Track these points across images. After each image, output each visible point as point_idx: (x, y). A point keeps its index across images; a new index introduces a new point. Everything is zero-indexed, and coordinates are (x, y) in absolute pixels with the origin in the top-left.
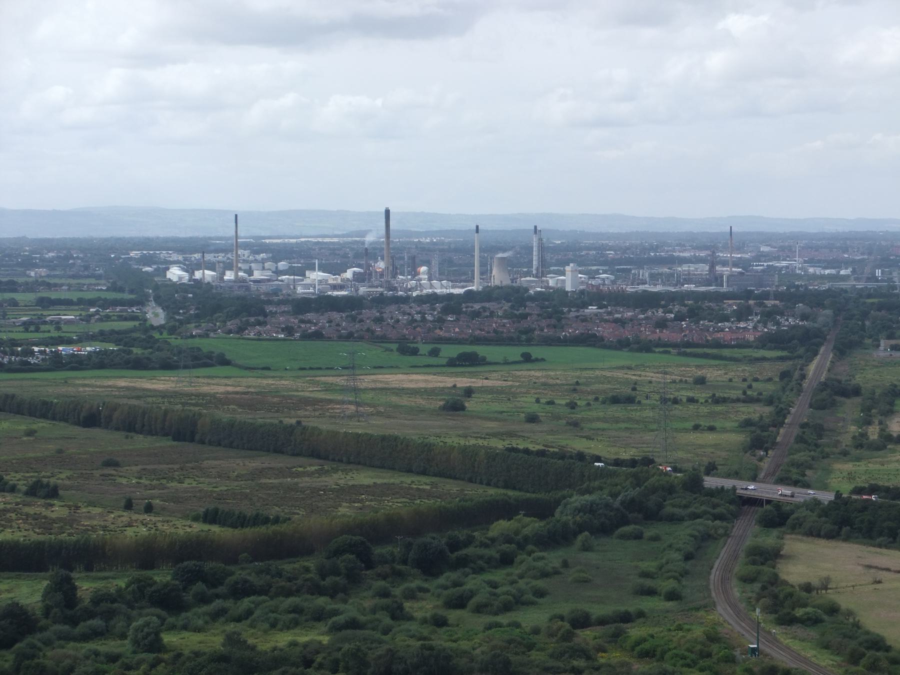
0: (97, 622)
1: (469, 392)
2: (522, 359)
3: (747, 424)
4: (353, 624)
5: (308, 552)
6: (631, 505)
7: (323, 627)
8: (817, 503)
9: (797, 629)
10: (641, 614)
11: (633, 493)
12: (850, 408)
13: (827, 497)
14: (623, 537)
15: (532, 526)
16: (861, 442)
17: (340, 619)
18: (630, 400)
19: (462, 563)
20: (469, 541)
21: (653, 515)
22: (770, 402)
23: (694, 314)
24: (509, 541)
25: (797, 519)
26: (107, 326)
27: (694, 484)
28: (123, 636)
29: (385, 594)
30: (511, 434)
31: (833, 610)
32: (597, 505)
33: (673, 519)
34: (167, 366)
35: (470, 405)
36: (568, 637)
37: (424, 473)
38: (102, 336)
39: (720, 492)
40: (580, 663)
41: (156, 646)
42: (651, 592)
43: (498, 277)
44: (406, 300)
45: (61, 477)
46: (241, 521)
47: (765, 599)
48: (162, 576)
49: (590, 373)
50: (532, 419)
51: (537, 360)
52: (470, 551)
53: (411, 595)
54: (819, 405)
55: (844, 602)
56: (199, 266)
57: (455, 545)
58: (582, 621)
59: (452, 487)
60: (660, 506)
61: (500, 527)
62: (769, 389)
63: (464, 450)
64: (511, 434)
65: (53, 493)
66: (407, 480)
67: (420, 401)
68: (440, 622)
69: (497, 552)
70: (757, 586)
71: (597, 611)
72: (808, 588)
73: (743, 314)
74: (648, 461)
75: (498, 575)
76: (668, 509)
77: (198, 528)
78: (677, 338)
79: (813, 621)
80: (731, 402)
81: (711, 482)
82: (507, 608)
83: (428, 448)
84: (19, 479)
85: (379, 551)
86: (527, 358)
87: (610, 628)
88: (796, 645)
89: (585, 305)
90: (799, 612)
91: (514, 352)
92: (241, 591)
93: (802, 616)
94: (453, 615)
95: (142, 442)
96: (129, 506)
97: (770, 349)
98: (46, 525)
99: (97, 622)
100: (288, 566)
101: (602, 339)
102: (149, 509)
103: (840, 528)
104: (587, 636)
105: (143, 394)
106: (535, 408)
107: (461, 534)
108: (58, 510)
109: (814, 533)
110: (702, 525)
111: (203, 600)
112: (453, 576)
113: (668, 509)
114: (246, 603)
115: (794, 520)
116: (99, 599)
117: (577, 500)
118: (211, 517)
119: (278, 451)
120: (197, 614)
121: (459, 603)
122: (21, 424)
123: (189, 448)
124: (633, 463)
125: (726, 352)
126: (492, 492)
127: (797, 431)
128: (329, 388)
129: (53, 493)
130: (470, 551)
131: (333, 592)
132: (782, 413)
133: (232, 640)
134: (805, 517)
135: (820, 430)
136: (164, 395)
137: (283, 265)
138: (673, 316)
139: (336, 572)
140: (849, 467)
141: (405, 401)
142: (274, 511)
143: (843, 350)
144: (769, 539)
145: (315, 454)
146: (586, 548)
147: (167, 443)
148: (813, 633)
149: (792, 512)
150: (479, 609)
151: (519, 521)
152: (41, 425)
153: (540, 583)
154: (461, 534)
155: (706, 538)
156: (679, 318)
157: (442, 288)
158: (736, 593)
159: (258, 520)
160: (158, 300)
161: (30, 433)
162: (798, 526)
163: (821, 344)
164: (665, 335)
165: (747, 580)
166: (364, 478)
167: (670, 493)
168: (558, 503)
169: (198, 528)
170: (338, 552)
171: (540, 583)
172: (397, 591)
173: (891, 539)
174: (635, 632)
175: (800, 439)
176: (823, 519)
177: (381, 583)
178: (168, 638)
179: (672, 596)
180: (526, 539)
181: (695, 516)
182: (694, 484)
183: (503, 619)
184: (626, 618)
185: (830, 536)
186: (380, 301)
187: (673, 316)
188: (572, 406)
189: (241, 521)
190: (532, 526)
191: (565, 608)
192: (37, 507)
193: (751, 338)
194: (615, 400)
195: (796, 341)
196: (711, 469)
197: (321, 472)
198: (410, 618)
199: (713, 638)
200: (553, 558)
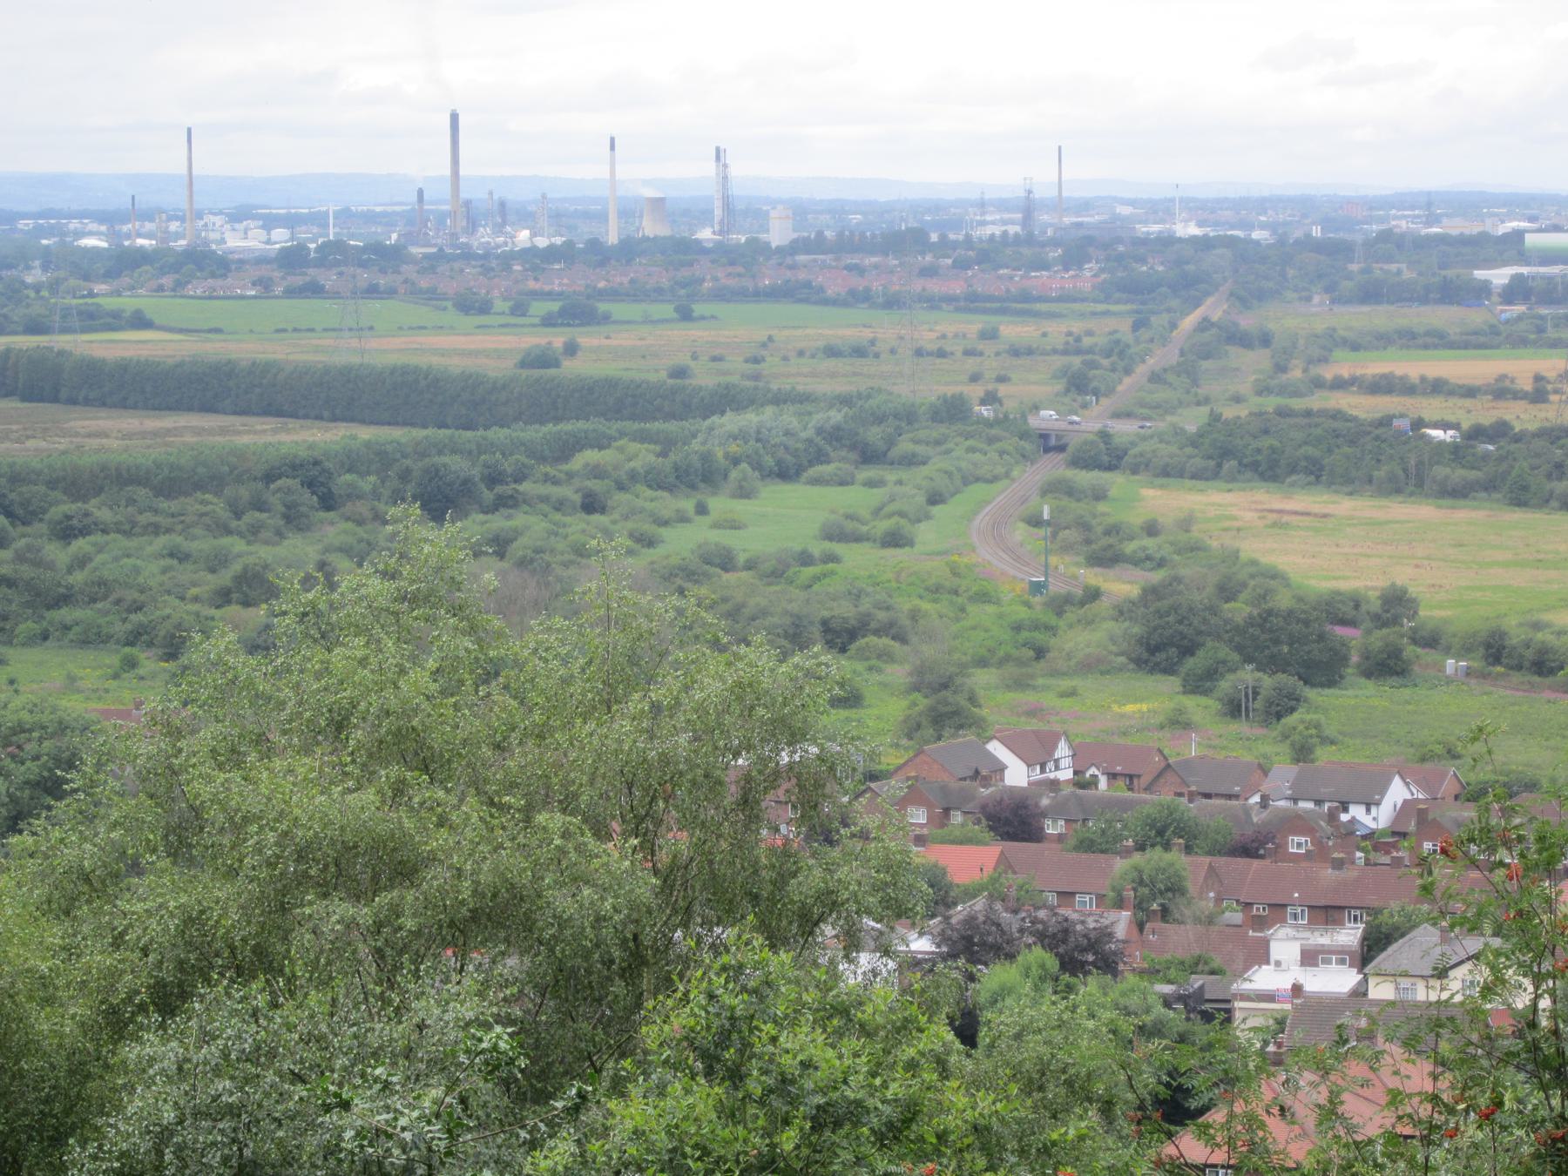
2: (675, 315)
6: (835, 435)
8: (1178, 431)
14: (817, 481)
25: (1141, 455)
32: (769, 430)
33: (910, 461)
47: (1067, 531)
49: (799, 332)
51: (703, 318)
60: (891, 442)
69: (576, 492)
78: (957, 288)
80: (1041, 354)
93: (1135, 552)
97: (1118, 302)
101: (821, 289)
103: (1219, 465)
113: (904, 446)
115: (1135, 456)
125: (1039, 306)
134: (1154, 451)
138: (950, 261)
149: (1133, 444)
151: (621, 450)
162: (1143, 467)
163: (1208, 294)
164: (934, 287)
167: (910, 423)
173: (1312, 478)
176: (1189, 450)
180: (633, 476)
187: (950, 261)
195: (1164, 289)
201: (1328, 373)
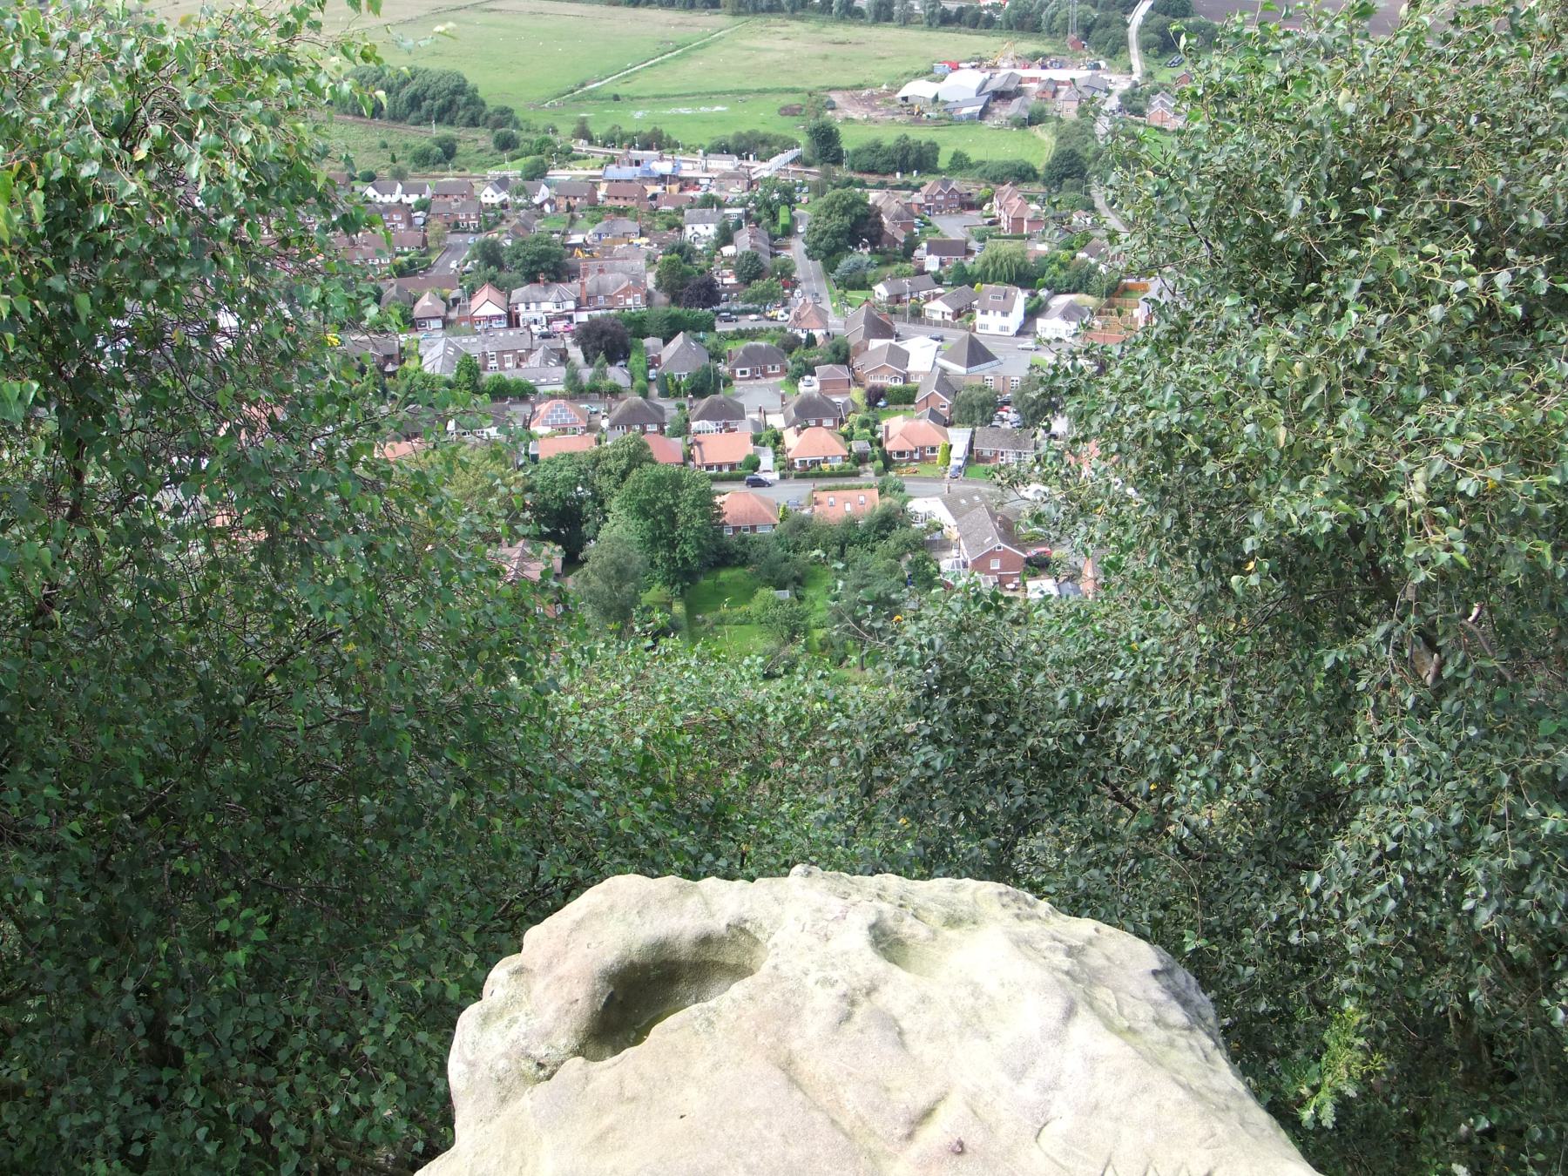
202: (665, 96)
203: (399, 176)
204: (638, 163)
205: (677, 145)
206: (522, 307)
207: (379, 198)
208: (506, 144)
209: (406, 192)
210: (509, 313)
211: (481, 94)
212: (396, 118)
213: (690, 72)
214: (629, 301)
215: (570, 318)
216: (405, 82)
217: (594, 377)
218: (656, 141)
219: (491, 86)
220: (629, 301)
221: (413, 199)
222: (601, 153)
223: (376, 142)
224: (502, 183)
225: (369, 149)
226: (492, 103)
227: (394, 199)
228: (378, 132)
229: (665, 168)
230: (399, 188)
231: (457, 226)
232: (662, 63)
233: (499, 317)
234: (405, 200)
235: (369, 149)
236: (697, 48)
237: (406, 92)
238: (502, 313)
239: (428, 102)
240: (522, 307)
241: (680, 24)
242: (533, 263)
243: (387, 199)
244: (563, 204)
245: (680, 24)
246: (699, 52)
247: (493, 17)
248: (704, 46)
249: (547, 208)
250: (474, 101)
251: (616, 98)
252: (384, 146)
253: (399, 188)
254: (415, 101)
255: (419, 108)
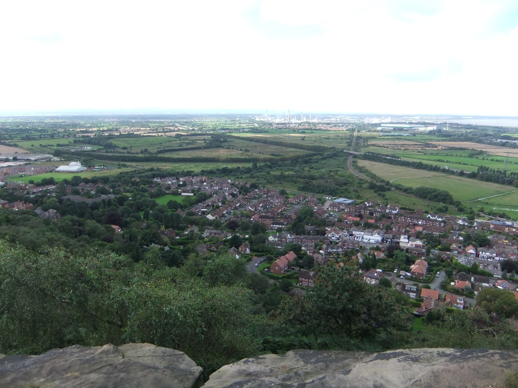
0: (260, 170)
1: (305, 137)
3: (347, 142)
4: (297, 171)
5: (288, 160)
7: (292, 171)
9: (363, 173)
10: (339, 170)
11: (334, 152)
12: (361, 140)
13: (363, 154)
15: (320, 157)
16: (364, 145)
17: (295, 170)
18: (328, 139)
19: (310, 162)
20: (311, 159)
21: (337, 156)
22: (349, 139)
23: (335, 126)
24: (317, 159)
26: (249, 127)
27: (342, 151)
28: (264, 172)
29: (300, 167)
30: (312, 143)
31: (367, 170)
34: (260, 133)
35: (305, 139)
36: (329, 174)
37: (301, 149)
38: (250, 128)
39: (346, 152)
40: (333, 177)
41: (269, 174)
42: (339, 167)
43: (305, 120)
44: (292, 123)
45: (249, 149)
46: (277, 156)
48: (269, 164)
50: (315, 141)
52: (312, 160)
53: (304, 167)
54: (357, 140)
55: (368, 169)
56: (261, 118)
57: (310, 160)
58: (331, 171)
59: (306, 151)
61: (315, 157)
62: (349, 137)
63: (308, 146)
64: (312, 143)
65: (248, 151)
66: (299, 150)
67: (297, 138)
68: (310, 171)
70: (355, 167)
71: (333, 170)
72: (362, 167)
73: (343, 126)
74: (335, 148)
75: (316, 164)
76: (339, 155)
77: (270, 156)
79: (364, 172)
81: (345, 151)
82: (319, 169)
83: (302, 145)
84: (244, 149)
85: (299, 160)
86: (312, 132)
87: (335, 172)
88: (362, 175)
89: (319, 124)
90: (362, 171)
91: (310, 131)
92: (280, 166)
94: (311, 170)
95: (259, 144)
96: (260, 153)
98: (249, 156)
99: (260, 170)
100: (286, 162)
102: (263, 154)
104: (332, 173)
105: (257, 137)
106: (315, 140)
107: (310, 158)
108: (249, 154)
109: (361, 159)
110: (345, 157)
111: (274, 167)
112: (310, 164)
114: (281, 167)
116: (260, 167)
117: (326, 153)
118: (272, 155)
119: (279, 145)
120: (274, 169)
121: (312, 168)
122: (241, 141)
123: (266, 145)
124: (332, 148)
126: (314, 152)
127: (354, 144)
128: (284, 136)
129: (248, 151)
130: (312, 160)
131: (293, 166)
132: (352, 141)
133: (282, 173)
135: (358, 143)
136: (260, 137)
137: (272, 118)
139: (293, 163)
140: (363, 149)
141: (295, 138)
142: (281, 154)
143: (359, 131)
144: (355, 159)
145: (285, 146)
146: (328, 160)
147: (262, 144)
148: (365, 174)
150: (315, 169)
152: (244, 141)
153: (323, 166)
154: (310, 158)
155: (346, 159)
156: (333, 126)
157: (297, 121)
158: (352, 168)
159: (279, 155)
160: (256, 123)
161: (243, 142)
164: (332, 129)
165: (353, 166)
166: (293, 149)
168: (323, 154)
169: (270, 156)
170: (293, 160)
171: (323, 166)
172: (302, 166)
174: (339, 173)
175: (355, 145)
177: (299, 165)
178: (271, 173)
179: (343, 168)
181: (343, 156)
182: (342, 151)
183: (319, 171)
184: (337, 171)
185: (364, 159)
186: (288, 123)
188: (320, 139)
189: (277, 156)
190: (320, 157)
191: (328, 169)
192: (246, 153)
193: (344, 129)
194: (327, 139)
196: (344, 149)
197: (286, 149)
198: (305, 170)
199: (351, 174)
200: (324, 162)
201: (369, 143)
202: (501, 205)
203: (436, 213)
204: (499, 221)
205: (510, 218)
206: (481, 253)
207: (431, 218)
208: (461, 210)
209: (439, 218)
210: (477, 253)
211: (453, 197)
212: (430, 199)
213: (507, 200)
214: (512, 257)
215: (494, 258)
216: (434, 192)
217: (510, 276)
218: (503, 216)
219: (456, 196)
220: (512, 257)
221: (440, 219)
222: (487, 217)
223: (426, 204)
224: (464, 220)
225: (425, 206)
226: (455, 200)
227: (435, 218)
228: (426, 202)
229: (509, 223)
230: (437, 216)
231: (453, 228)
232: (498, 196)
233: (474, 254)
234: (438, 219)
235: (425, 206)
236: (507, 194)
237: (434, 194)
238: (475, 253)
239: (440, 197)
240: (481, 253)
241: (501, 187)
242: (481, 242)
243: (433, 218)
244: (481, 228)
245: (501, 187)
246: (509, 195)
247: (448, 179)
248: (509, 194)
249: (476, 228)
250: (451, 197)
251: (487, 203)
252: (428, 205)
253: (437, 216)
254: (436, 196)
255: (437, 198)
